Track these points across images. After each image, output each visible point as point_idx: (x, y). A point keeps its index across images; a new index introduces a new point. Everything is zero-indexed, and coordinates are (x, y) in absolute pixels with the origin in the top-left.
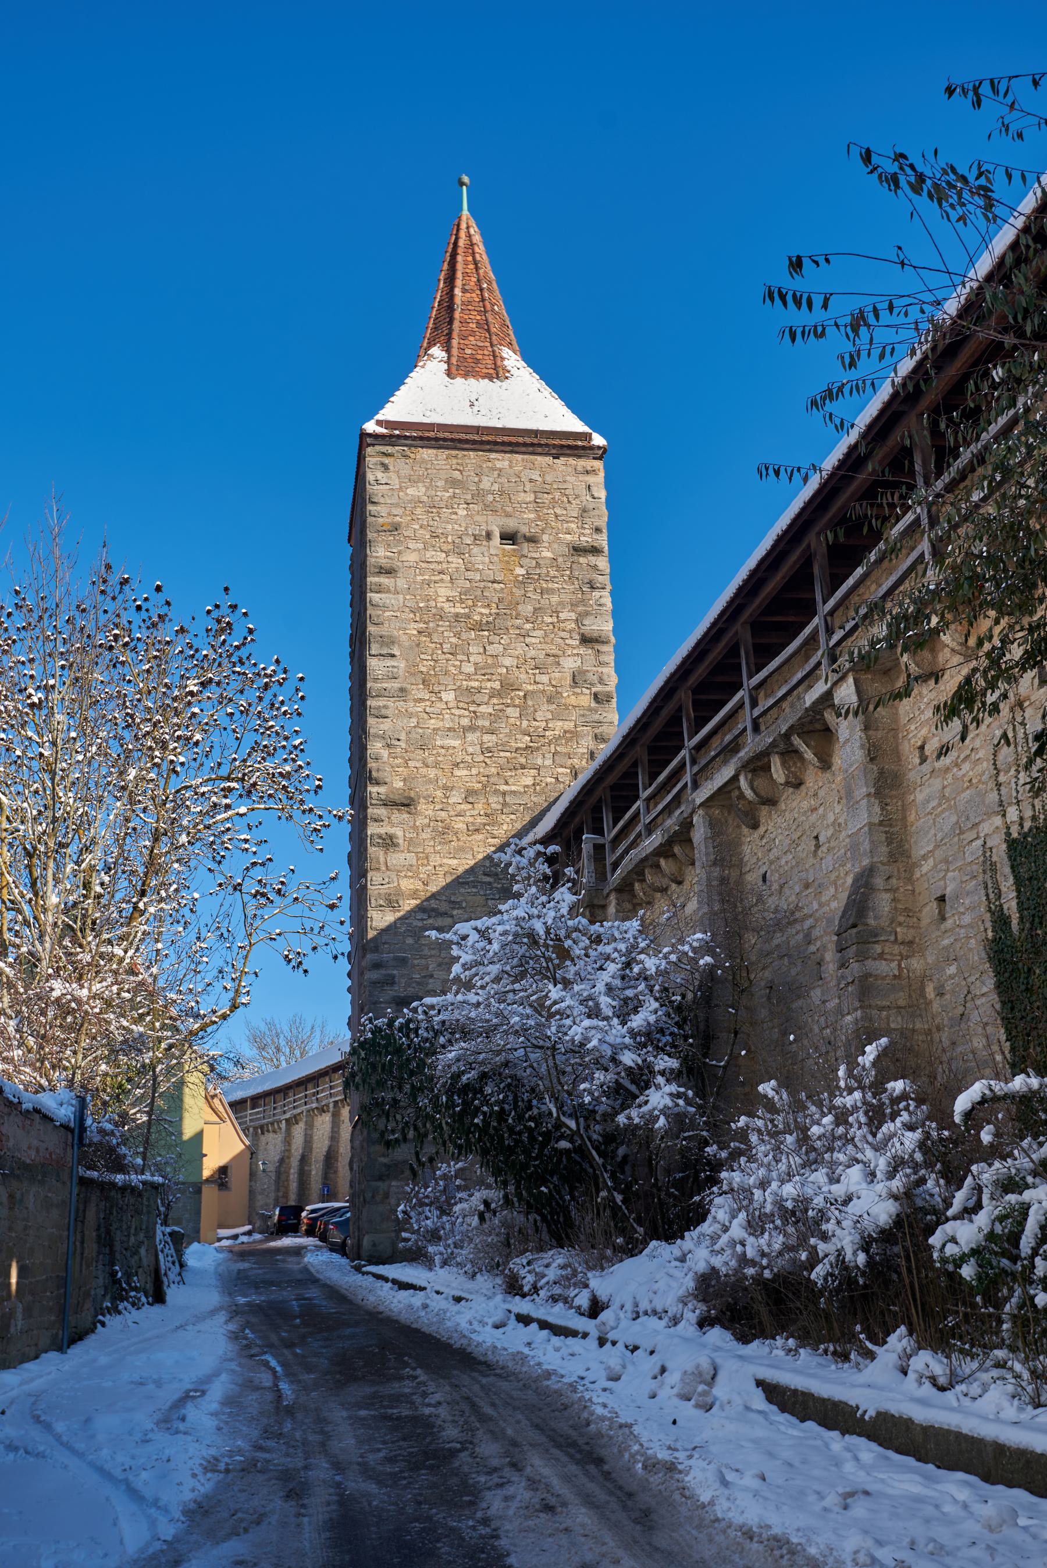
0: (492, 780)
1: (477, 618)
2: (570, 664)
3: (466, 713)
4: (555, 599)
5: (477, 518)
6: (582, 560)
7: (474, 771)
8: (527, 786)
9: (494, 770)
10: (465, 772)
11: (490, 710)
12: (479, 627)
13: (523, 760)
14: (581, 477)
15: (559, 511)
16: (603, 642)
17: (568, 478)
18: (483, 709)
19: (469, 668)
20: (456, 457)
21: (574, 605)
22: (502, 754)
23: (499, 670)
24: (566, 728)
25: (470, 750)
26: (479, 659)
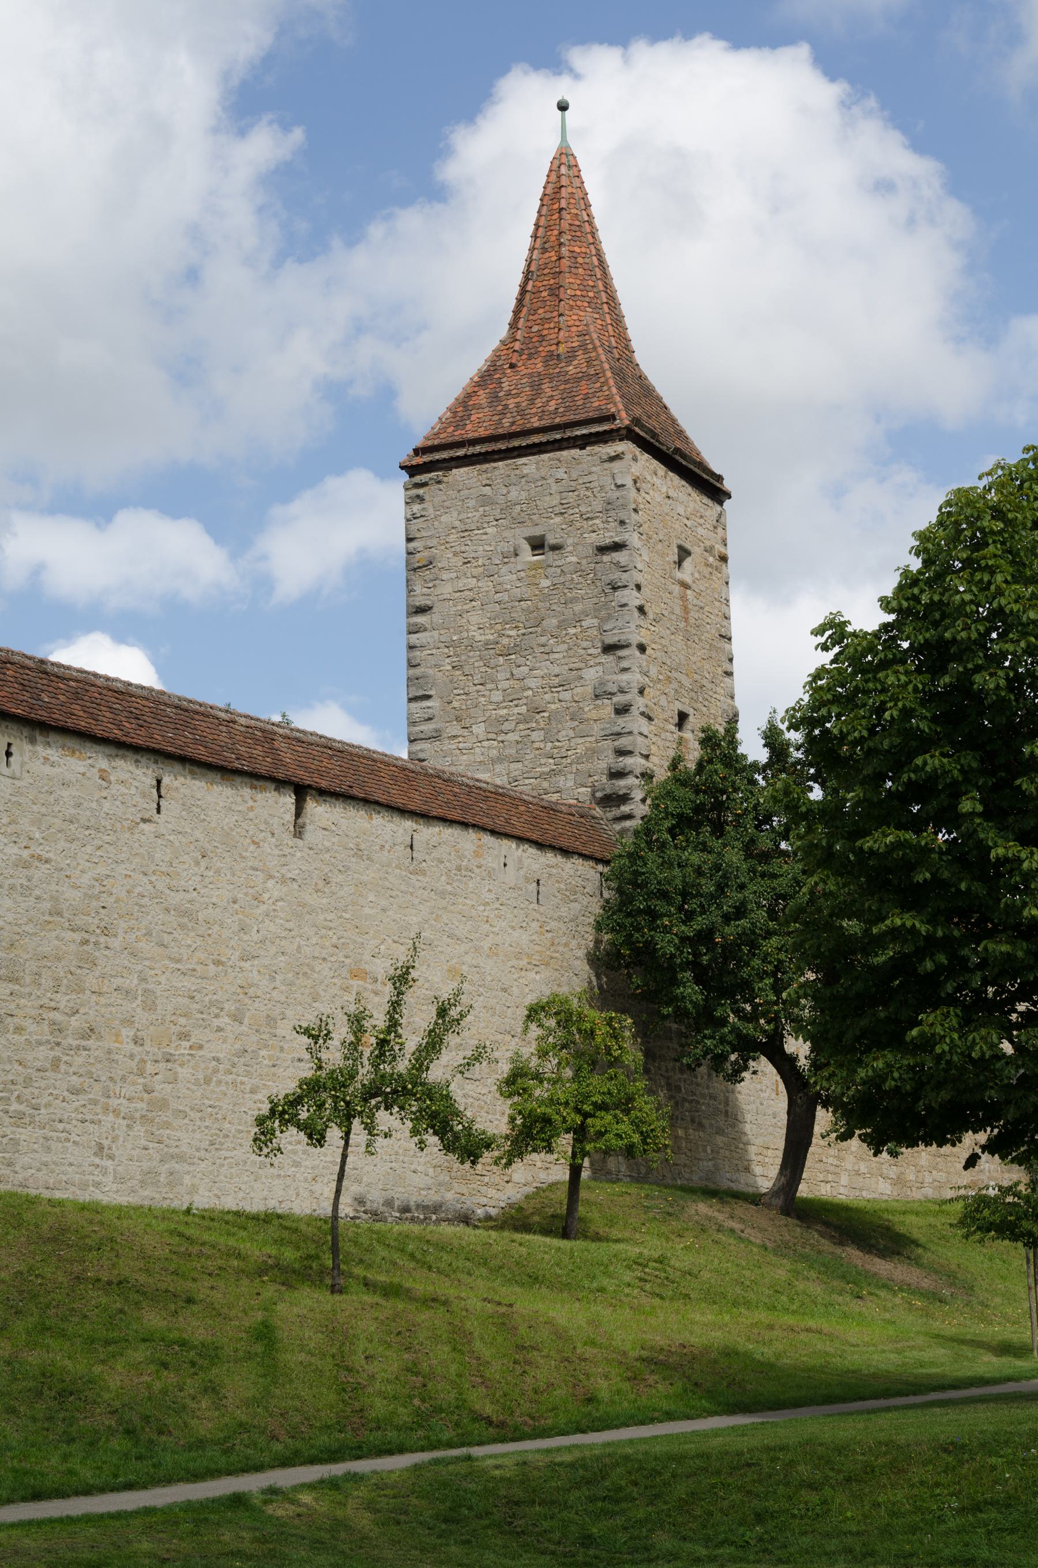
1: (505, 641)
2: (591, 675)
4: (578, 608)
5: (507, 534)
6: (606, 558)
13: (545, 785)
14: (607, 465)
15: (583, 509)
17: (594, 469)
18: (512, 737)
19: (497, 697)
22: (527, 781)
23: (525, 694)
24: (588, 745)
26: (505, 684)
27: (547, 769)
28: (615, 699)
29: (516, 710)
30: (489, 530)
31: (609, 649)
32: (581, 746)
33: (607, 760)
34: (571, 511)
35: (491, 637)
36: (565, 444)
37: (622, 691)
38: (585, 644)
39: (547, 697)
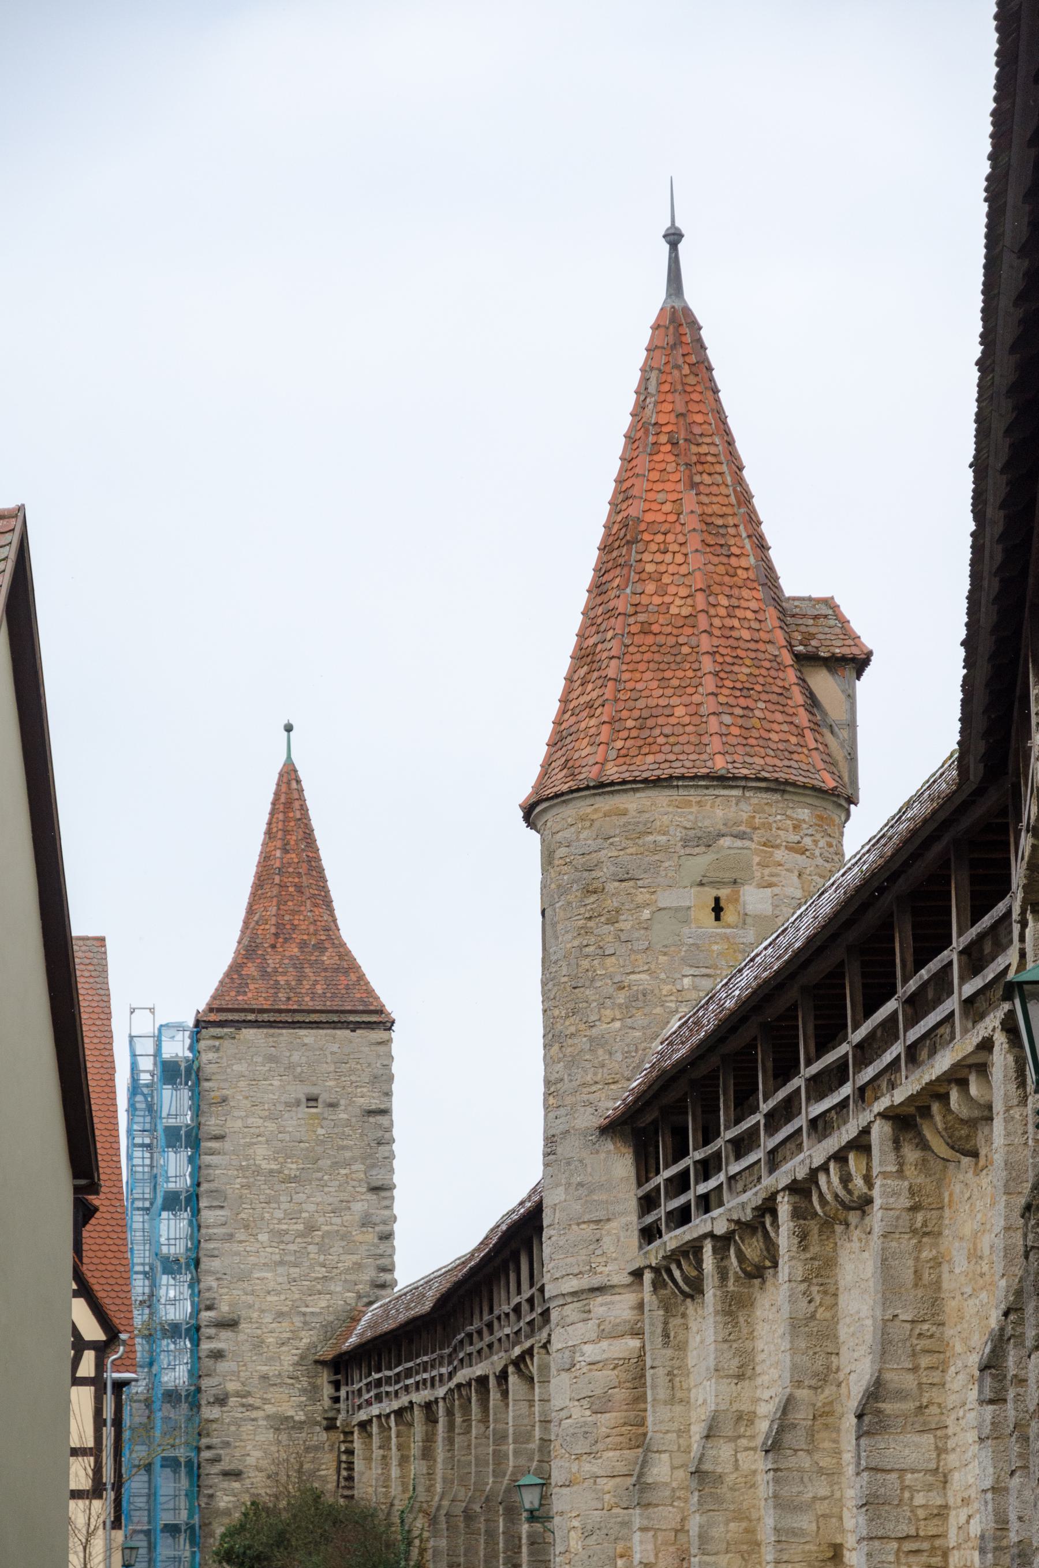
0: (296, 1304)
2: (358, 1207)
3: (277, 1250)
4: (348, 1154)
6: (372, 1120)
7: (283, 1297)
8: (323, 1308)
9: (297, 1296)
10: (276, 1298)
11: (296, 1248)
12: (290, 1179)
13: (319, 1287)
14: (373, 1048)
16: (386, 1189)
18: (292, 1247)
19: (279, 1214)
20: (272, 1036)
21: (364, 1158)
25: (280, 1280)
27: (320, 1276)
28: (377, 1229)
29: (295, 1227)
30: (276, 1083)
31: (375, 1189)
32: (349, 1260)
33: (369, 1274)
34: (343, 1079)
35: (275, 1167)
36: (339, 1025)
37: (384, 1223)
38: (354, 1183)
39: (322, 1220)
